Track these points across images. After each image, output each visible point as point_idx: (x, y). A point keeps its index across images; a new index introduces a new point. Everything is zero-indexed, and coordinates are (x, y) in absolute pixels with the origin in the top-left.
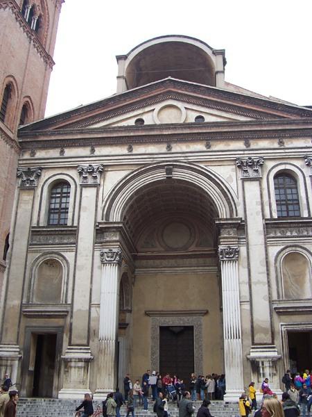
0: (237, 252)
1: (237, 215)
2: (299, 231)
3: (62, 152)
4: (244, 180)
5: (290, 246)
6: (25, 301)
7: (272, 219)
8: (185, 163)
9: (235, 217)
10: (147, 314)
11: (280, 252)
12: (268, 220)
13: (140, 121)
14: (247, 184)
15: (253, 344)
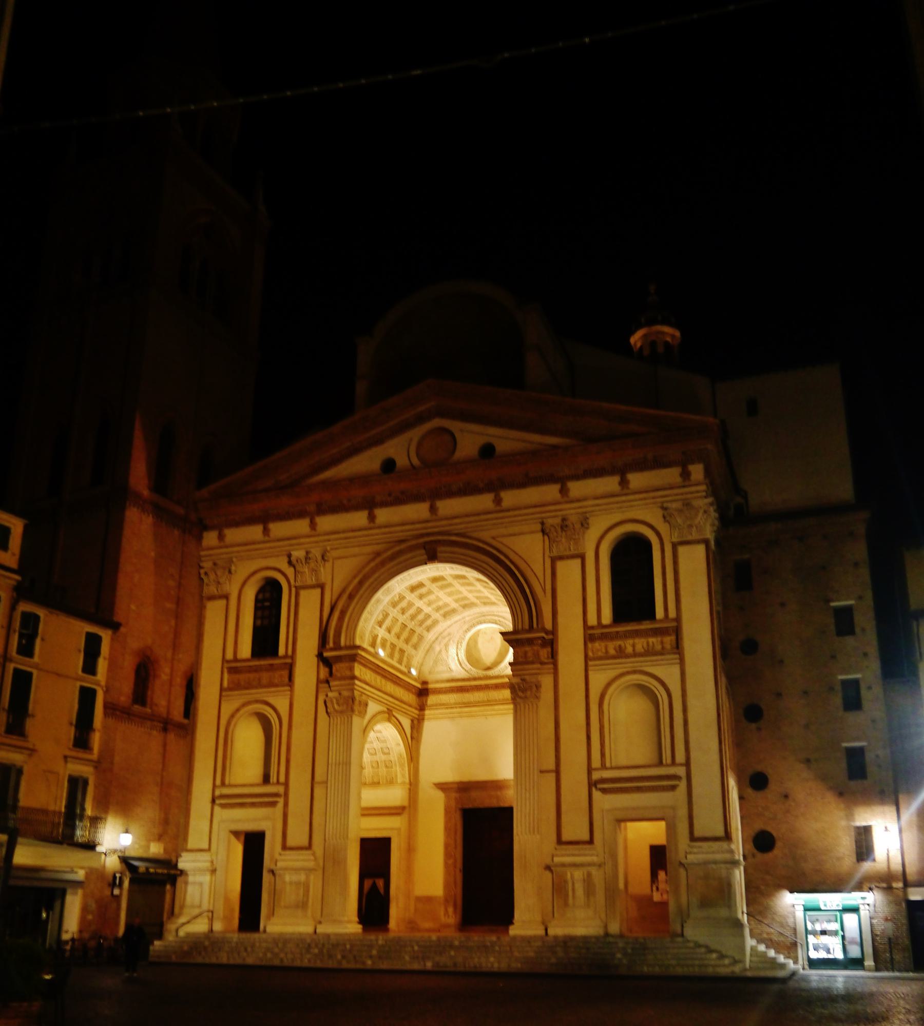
0: (538, 687)
1: (537, 625)
2: (648, 643)
3: (266, 531)
4: (554, 561)
5: (628, 673)
6: (218, 782)
7: (600, 625)
8: (457, 535)
9: (535, 625)
10: (442, 787)
11: (608, 685)
12: (592, 628)
13: (389, 466)
14: (560, 565)
15: (560, 841)
